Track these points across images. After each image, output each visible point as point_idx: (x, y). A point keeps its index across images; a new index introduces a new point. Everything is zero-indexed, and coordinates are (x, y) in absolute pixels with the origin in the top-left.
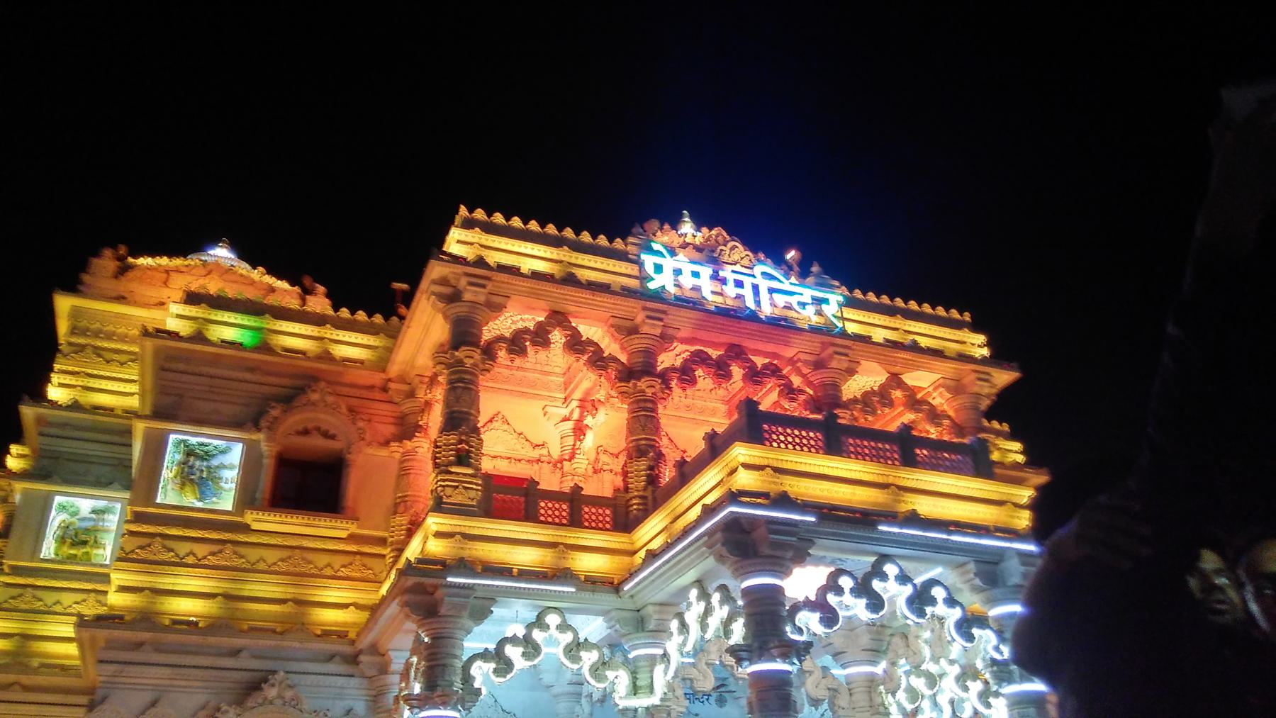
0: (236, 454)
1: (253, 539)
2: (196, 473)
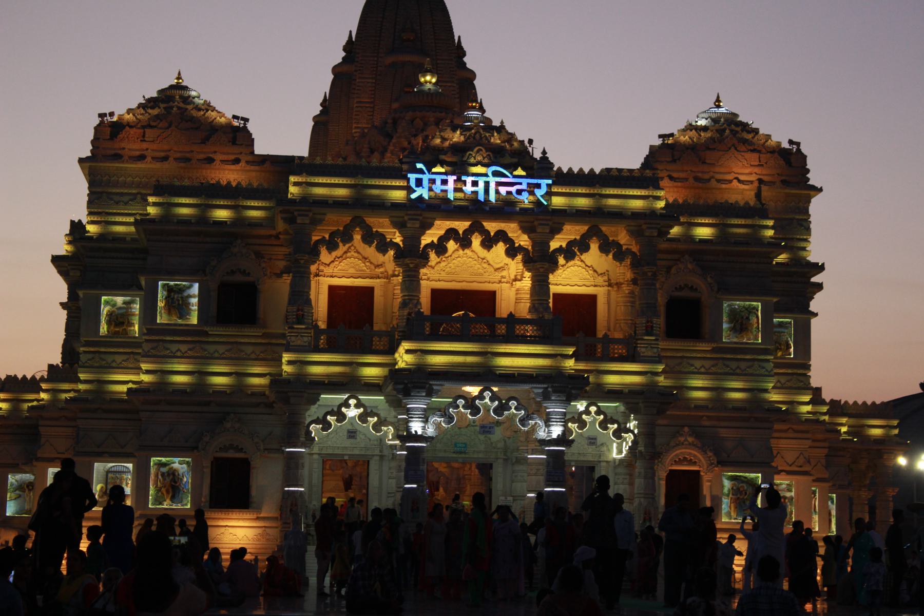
0: (195, 289)
1: (210, 340)
2: (177, 303)
